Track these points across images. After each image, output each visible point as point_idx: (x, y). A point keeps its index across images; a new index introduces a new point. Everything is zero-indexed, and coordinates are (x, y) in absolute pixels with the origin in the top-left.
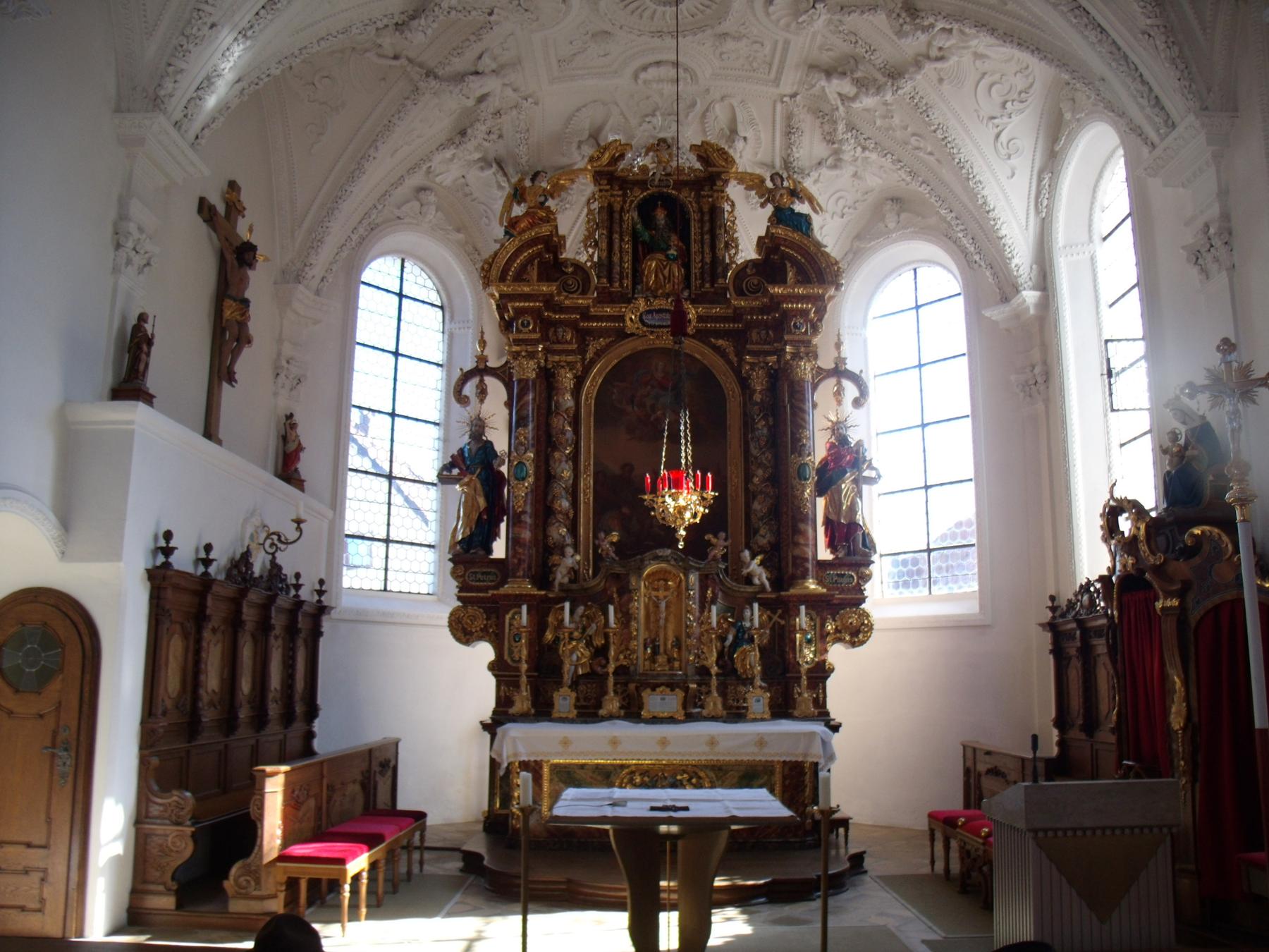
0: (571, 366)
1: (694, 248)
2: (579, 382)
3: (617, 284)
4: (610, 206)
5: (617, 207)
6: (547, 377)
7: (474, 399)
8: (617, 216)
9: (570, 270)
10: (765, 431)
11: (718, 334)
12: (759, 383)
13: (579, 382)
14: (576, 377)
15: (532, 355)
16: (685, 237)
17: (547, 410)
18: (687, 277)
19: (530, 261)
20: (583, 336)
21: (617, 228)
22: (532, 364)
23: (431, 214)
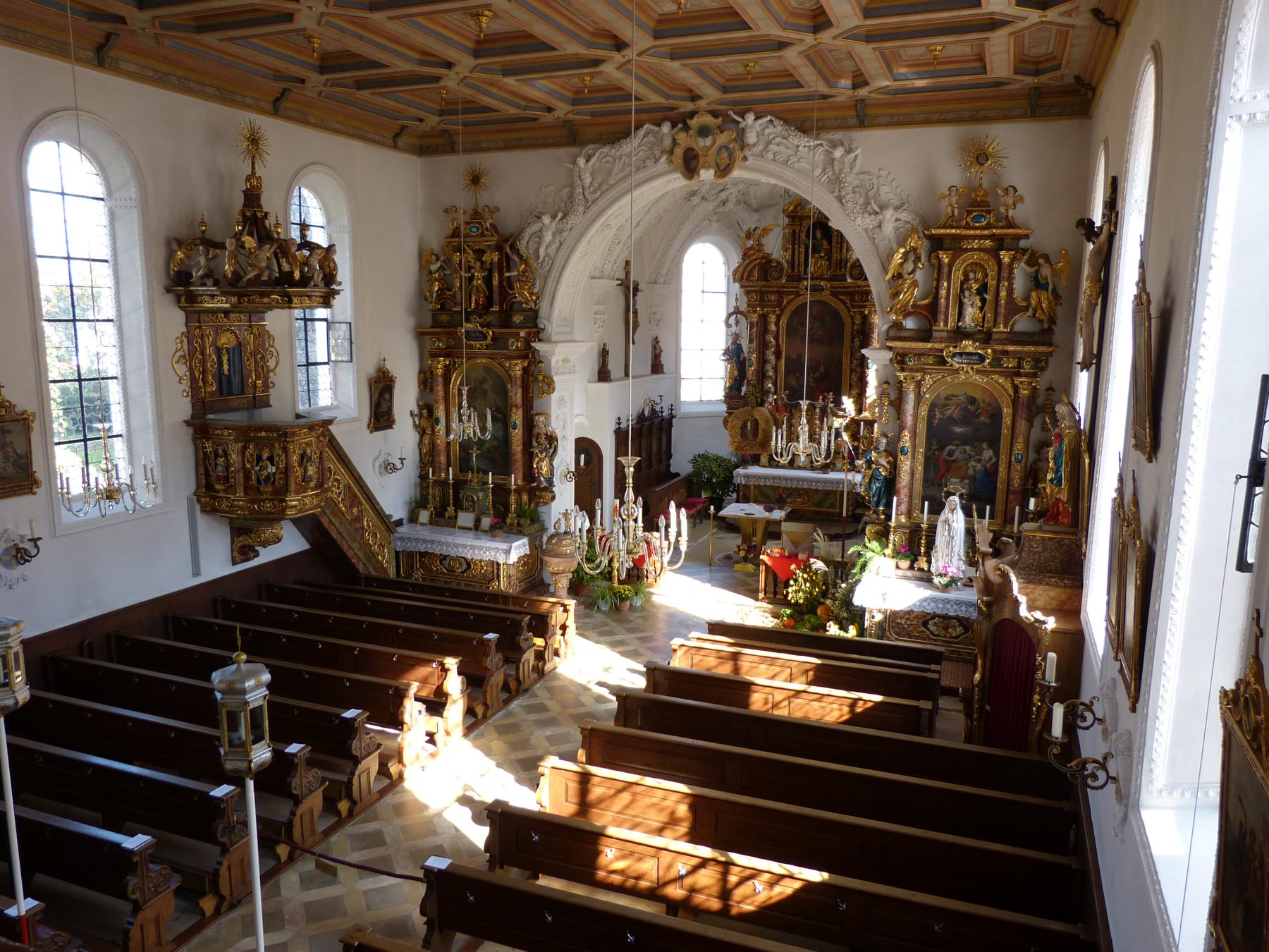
0: (774, 312)
1: (834, 250)
2: (778, 317)
3: (796, 271)
4: (794, 231)
5: (797, 231)
6: (764, 318)
7: (734, 326)
8: (797, 235)
9: (775, 264)
10: (858, 343)
11: (843, 294)
12: (858, 320)
13: (778, 317)
14: (777, 316)
15: (755, 312)
16: (830, 243)
17: (765, 330)
18: (830, 264)
19: (754, 267)
20: (780, 295)
21: (797, 242)
22: (755, 316)
23: (715, 225)
